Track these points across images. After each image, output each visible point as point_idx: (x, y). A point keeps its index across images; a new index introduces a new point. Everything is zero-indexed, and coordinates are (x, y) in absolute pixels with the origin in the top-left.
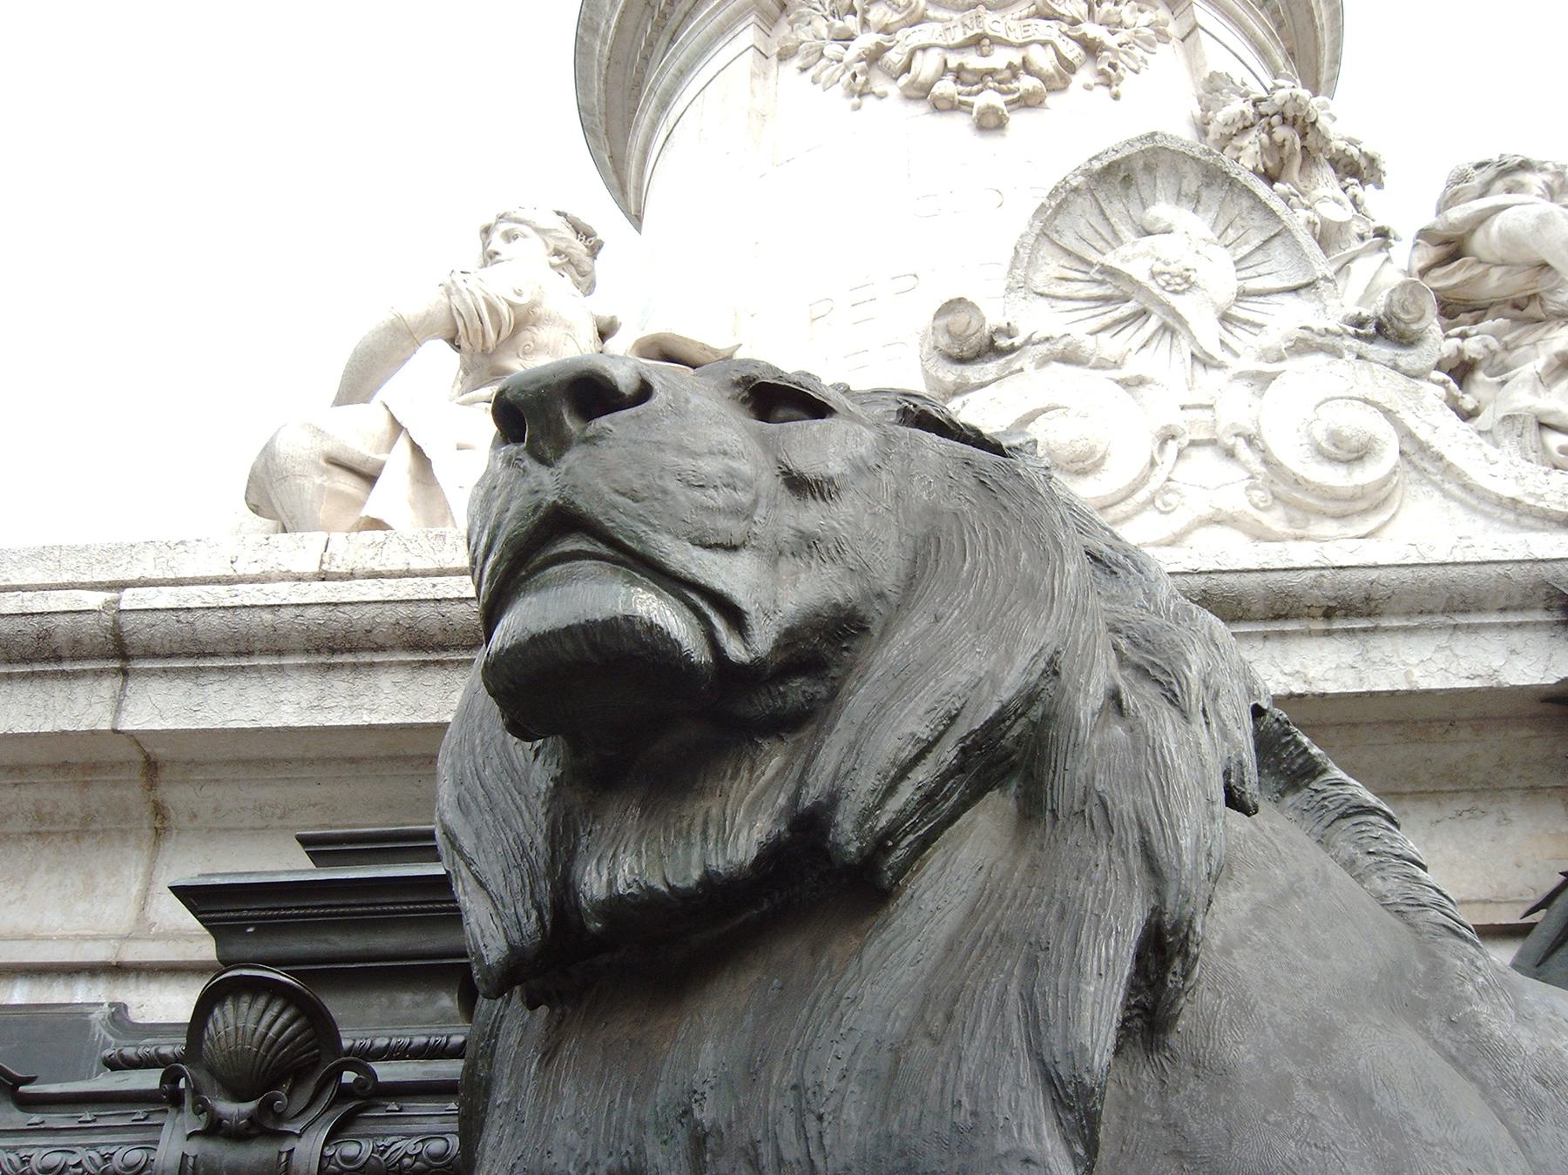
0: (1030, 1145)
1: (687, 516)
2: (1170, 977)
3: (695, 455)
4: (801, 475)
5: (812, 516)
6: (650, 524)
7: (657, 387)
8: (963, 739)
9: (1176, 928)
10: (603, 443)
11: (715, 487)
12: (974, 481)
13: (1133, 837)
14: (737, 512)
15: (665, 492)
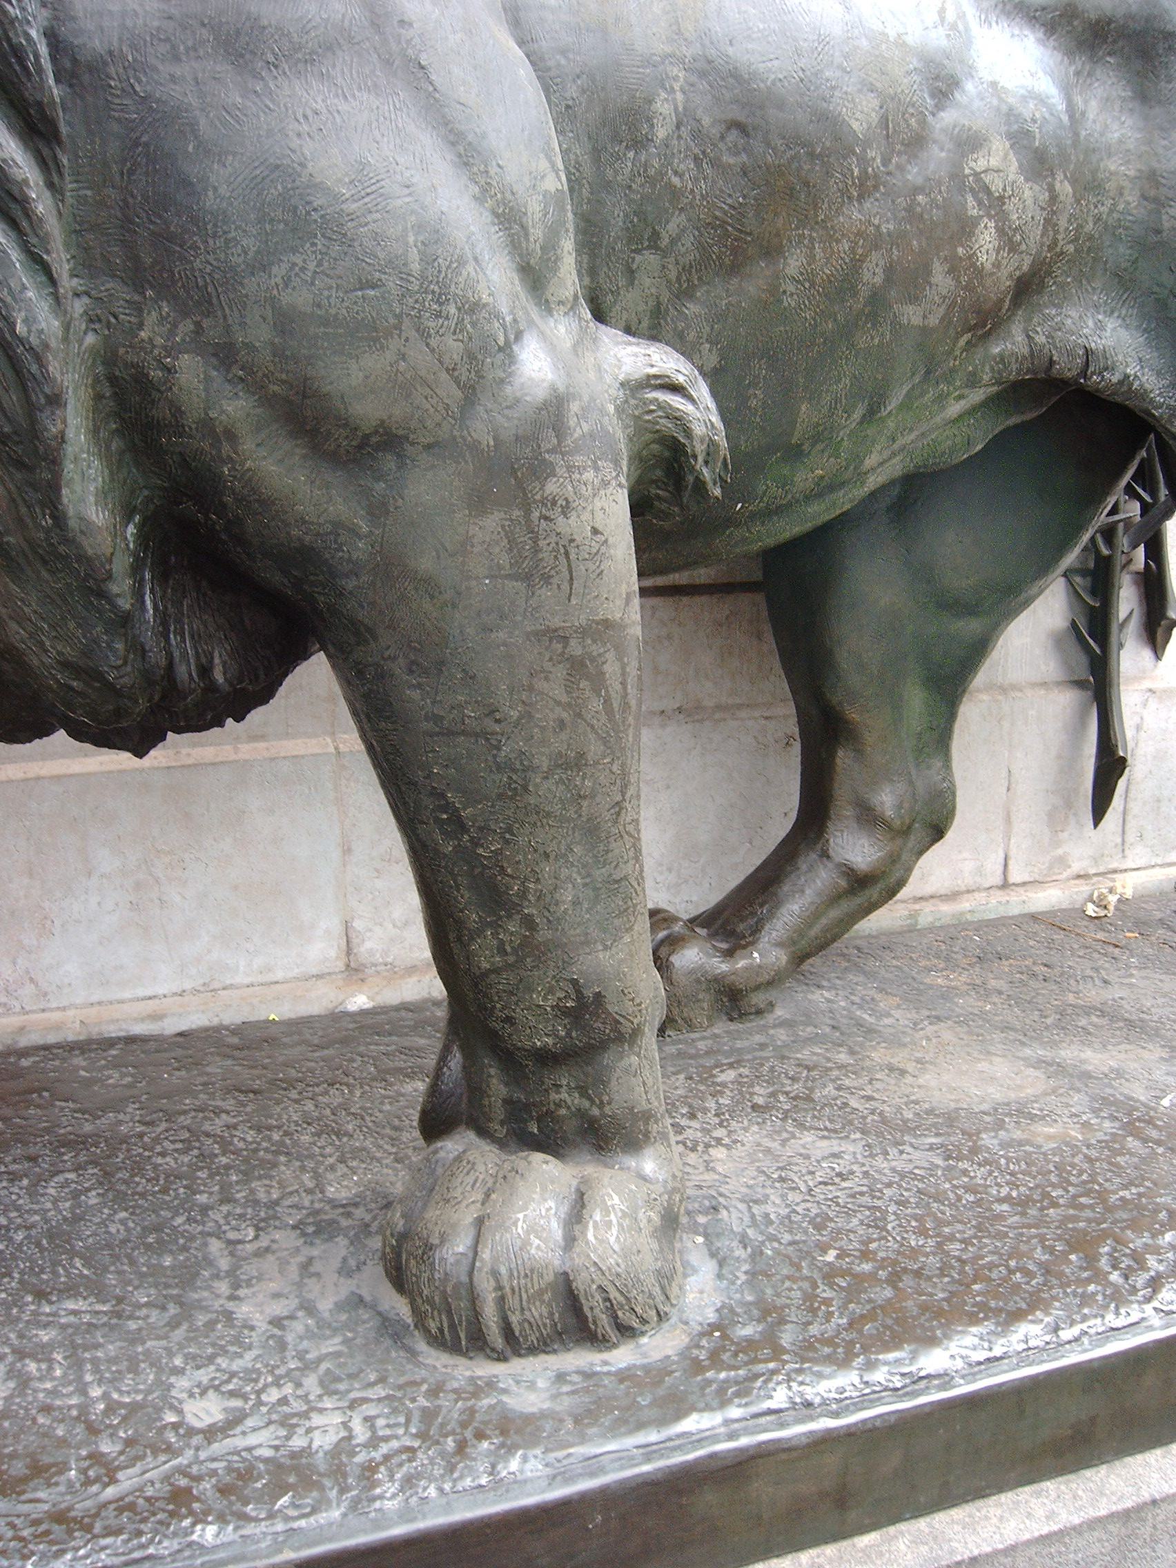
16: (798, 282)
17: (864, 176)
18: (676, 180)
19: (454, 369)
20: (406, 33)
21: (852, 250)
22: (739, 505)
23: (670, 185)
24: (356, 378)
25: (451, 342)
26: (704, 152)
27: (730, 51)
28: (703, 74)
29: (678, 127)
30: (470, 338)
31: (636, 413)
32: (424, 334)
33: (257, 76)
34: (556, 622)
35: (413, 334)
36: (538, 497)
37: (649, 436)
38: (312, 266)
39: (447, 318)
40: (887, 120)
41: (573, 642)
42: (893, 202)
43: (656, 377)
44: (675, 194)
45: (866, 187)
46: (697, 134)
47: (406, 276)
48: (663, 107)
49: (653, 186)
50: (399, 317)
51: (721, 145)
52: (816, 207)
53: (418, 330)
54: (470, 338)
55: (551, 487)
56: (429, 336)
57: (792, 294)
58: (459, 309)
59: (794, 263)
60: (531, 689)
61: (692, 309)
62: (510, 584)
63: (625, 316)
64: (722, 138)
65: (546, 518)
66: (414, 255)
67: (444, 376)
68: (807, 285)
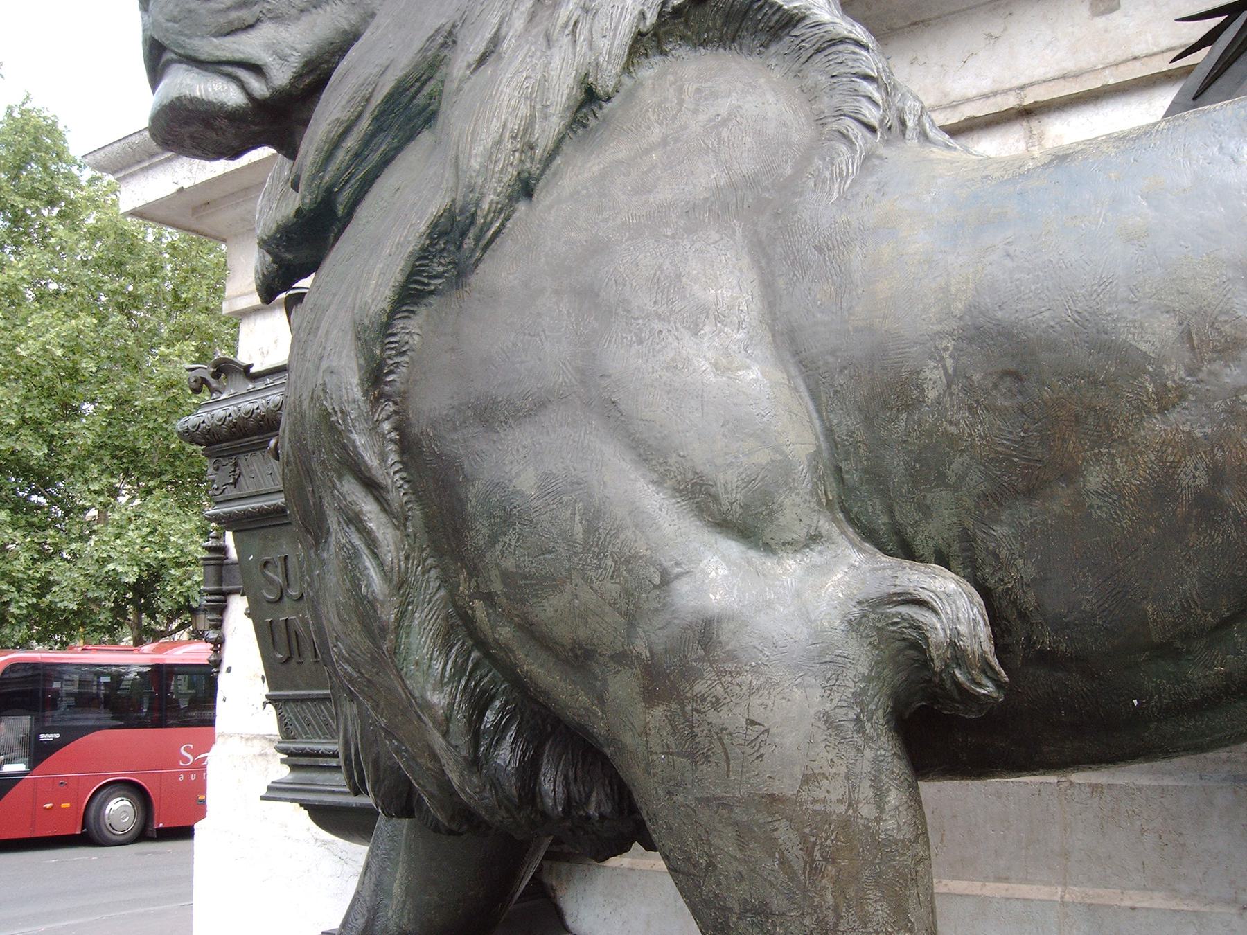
1: (207, 22)
2: (467, 241)
9: (462, 212)
13: (452, 153)
15: (190, 11)
16: (1104, 495)
17: (1162, 391)
18: (953, 429)
21: (1160, 458)
22: (1135, 701)
23: (946, 434)
24: (550, 612)
25: (609, 585)
26: (977, 402)
27: (999, 314)
28: (971, 340)
29: (949, 386)
31: (879, 625)
32: (589, 582)
34: (719, 792)
35: (579, 581)
36: (689, 695)
37: (898, 644)
38: (513, 543)
39: (605, 569)
40: (1190, 333)
42: (1208, 406)
43: (895, 594)
44: (952, 440)
45: (1166, 400)
46: (969, 389)
47: (570, 542)
48: (933, 375)
49: (930, 436)
50: (569, 570)
51: (994, 393)
52: (1108, 427)
55: (700, 687)
56: (592, 581)
57: (1100, 508)
58: (616, 562)
59: (1095, 479)
60: (709, 843)
61: (999, 530)
62: (678, 760)
63: (931, 543)
64: (995, 386)
65: (698, 711)
66: (579, 529)
67: (607, 608)
68: (1115, 497)
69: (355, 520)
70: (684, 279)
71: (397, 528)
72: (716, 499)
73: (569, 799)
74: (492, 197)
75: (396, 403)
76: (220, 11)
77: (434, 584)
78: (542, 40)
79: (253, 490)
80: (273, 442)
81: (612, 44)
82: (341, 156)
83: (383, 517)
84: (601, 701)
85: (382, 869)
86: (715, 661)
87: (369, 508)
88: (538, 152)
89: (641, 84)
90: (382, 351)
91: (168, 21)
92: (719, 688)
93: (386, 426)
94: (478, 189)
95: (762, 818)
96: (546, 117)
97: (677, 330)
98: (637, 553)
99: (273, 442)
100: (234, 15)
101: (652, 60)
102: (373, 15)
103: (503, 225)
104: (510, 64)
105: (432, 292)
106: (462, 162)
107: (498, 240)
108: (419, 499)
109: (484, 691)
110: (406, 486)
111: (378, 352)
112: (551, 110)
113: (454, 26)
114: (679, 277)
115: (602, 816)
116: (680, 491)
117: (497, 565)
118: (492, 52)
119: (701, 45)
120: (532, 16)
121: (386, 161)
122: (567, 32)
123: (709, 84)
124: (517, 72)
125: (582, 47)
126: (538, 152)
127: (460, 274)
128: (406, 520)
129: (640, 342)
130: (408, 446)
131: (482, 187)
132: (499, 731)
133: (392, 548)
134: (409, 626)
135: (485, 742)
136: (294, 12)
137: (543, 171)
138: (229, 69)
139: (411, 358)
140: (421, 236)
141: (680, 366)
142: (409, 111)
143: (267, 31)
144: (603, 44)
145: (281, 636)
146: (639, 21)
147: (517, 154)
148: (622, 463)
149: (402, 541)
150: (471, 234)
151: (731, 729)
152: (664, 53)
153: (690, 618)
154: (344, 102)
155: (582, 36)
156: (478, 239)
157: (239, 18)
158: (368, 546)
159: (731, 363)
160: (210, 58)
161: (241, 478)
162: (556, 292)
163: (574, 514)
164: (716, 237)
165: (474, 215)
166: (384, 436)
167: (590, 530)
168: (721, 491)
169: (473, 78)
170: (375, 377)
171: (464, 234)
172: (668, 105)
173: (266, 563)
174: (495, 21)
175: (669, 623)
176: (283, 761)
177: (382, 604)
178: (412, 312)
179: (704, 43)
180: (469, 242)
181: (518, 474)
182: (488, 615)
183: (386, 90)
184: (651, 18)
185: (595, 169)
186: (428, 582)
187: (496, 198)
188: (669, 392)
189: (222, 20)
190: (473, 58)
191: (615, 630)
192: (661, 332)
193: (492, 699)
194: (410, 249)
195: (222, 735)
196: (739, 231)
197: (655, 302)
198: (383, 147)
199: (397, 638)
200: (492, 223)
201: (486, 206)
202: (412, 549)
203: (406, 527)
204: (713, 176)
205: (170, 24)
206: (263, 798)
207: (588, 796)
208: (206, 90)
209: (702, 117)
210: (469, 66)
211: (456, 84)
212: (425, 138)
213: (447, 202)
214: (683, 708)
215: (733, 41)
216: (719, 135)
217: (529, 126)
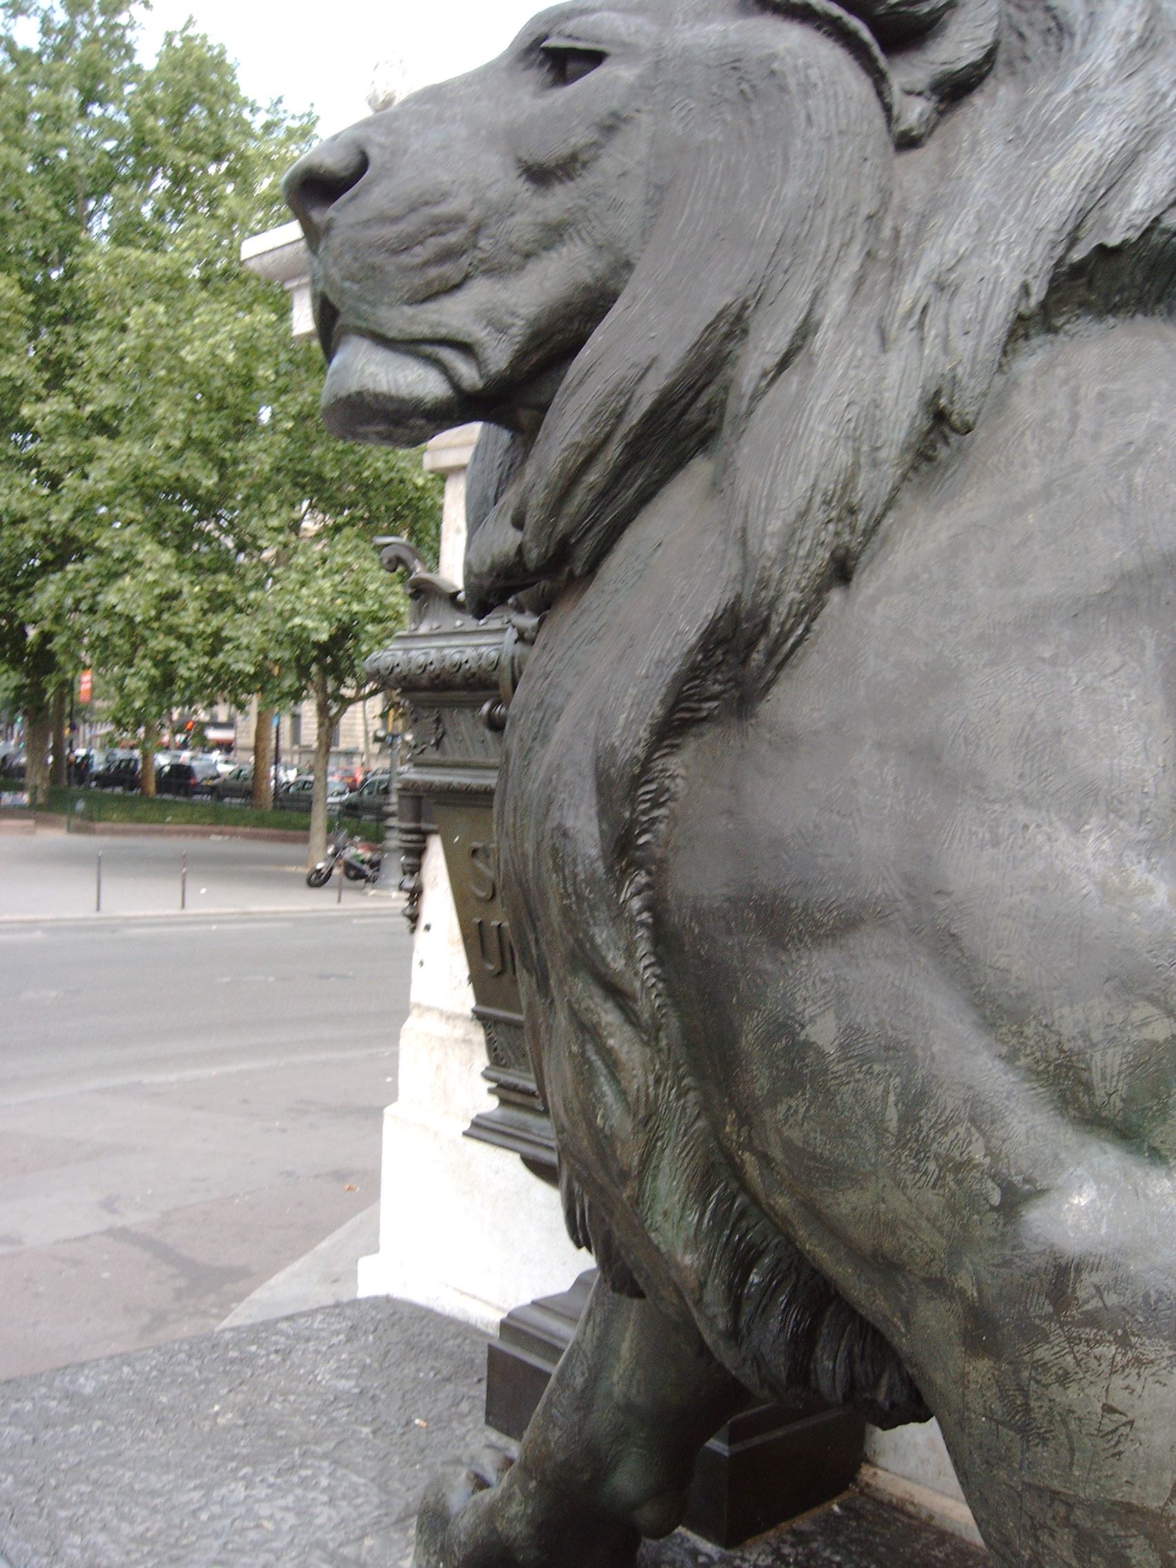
0: (569, 824)
1: (396, 284)
2: (755, 655)
3: (395, 220)
4: (541, 166)
5: (558, 201)
6: (368, 302)
7: (373, 153)
8: (626, 436)
9: (751, 614)
10: (333, 233)
11: (421, 243)
12: (736, 90)
13: (737, 522)
14: (447, 255)
15: (373, 268)
19: (936, 1219)
20: (941, 903)
24: (845, 1209)
30: (953, 1195)
32: (901, 1186)
33: (785, 948)
34: (1056, 1485)
35: (888, 1181)
39: (925, 1173)
41: (1079, 1513)
47: (880, 1131)
53: (894, 1179)
54: (953, 1195)
55: (1042, 1353)
56: (905, 1187)
62: (1004, 1430)
66: (892, 1116)
67: (924, 1224)
69: (588, 1030)
70: (1065, 740)
71: (647, 1044)
72: (1088, 1088)
73: (852, 1384)
74: (792, 595)
75: (649, 873)
76: (413, 268)
77: (692, 1111)
78: (873, 338)
79: (458, 758)
80: (486, 707)
81: (978, 344)
82: (581, 497)
83: (628, 1031)
84: (906, 1317)
85: (607, 1322)
86: (1067, 1323)
87: (608, 1016)
88: (862, 518)
89: (1016, 384)
90: (633, 811)
91: (344, 278)
92: (1069, 1358)
93: (636, 904)
94: (773, 584)
95: (1112, 1529)
96: (875, 464)
97: (1051, 824)
98: (970, 1160)
99: (486, 707)
100: (433, 272)
101: (1035, 341)
102: (628, 266)
103: (807, 629)
104: (825, 378)
105: (704, 719)
106: (752, 541)
107: (800, 650)
108: (677, 1004)
109: (750, 1247)
110: (660, 986)
111: (627, 814)
112: (883, 454)
113: (744, 307)
114: (1058, 733)
115: (893, 1405)
116: (1038, 1074)
117: (778, 1131)
118: (799, 348)
119: (1109, 312)
120: (860, 281)
121: (645, 498)
122: (911, 324)
123: (1117, 385)
124: (836, 395)
125: (931, 348)
126: (862, 518)
127: (744, 700)
128: (658, 1030)
129: (996, 843)
130: (664, 938)
131: (780, 580)
132: (768, 1292)
133: (639, 1072)
134: (657, 1167)
135: (748, 1308)
136: (516, 259)
137: (864, 545)
138: (428, 349)
139: (672, 811)
140: (690, 651)
141: (1051, 887)
142: (681, 428)
143: (480, 292)
144: (963, 346)
145: (493, 945)
146: (1020, 299)
147: (831, 527)
148: (959, 1026)
149: (652, 1060)
150: (762, 644)
151: (1080, 1412)
152: (1054, 330)
153: (1038, 1262)
154: (584, 420)
155: (931, 334)
156: (771, 654)
157: (440, 277)
158: (607, 1066)
159: (1126, 882)
160: (401, 337)
161: (445, 739)
162: (879, 745)
163: (886, 1092)
164: (1116, 660)
165: (766, 622)
166: (632, 919)
167: (909, 1118)
168: (1096, 1077)
169: (772, 391)
170: (623, 848)
171: (751, 645)
172: (1055, 424)
173: (474, 852)
174: (803, 299)
175: (1007, 1263)
176: (491, 1091)
177: (623, 1143)
178: (676, 746)
179: (1113, 310)
180: (757, 657)
181: (812, 1020)
182: (761, 1174)
183: (646, 404)
184: (1038, 292)
185: (943, 536)
186: (684, 1109)
187: (798, 596)
188: (1033, 927)
189: (418, 281)
190: (771, 361)
191: (933, 1251)
192: (1026, 827)
193: (761, 1254)
194: (675, 670)
195: (418, 1006)
196: (1150, 643)
197: (1021, 776)
198: (639, 482)
199: (640, 1185)
200: (792, 630)
201: (783, 609)
202: (664, 1067)
203: (657, 1039)
204: (1117, 555)
205: (347, 284)
206: (465, 1134)
207: (878, 1378)
208: (396, 381)
209: (1105, 448)
210: (764, 375)
211: (745, 403)
212: (700, 469)
213: (729, 596)
214: (1017, 1372)
215: (1159, 300)
216: (1129, 479)
217: (848, 484)
